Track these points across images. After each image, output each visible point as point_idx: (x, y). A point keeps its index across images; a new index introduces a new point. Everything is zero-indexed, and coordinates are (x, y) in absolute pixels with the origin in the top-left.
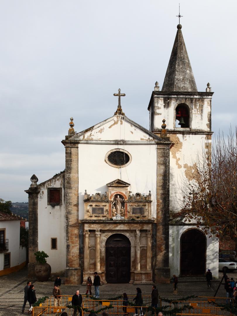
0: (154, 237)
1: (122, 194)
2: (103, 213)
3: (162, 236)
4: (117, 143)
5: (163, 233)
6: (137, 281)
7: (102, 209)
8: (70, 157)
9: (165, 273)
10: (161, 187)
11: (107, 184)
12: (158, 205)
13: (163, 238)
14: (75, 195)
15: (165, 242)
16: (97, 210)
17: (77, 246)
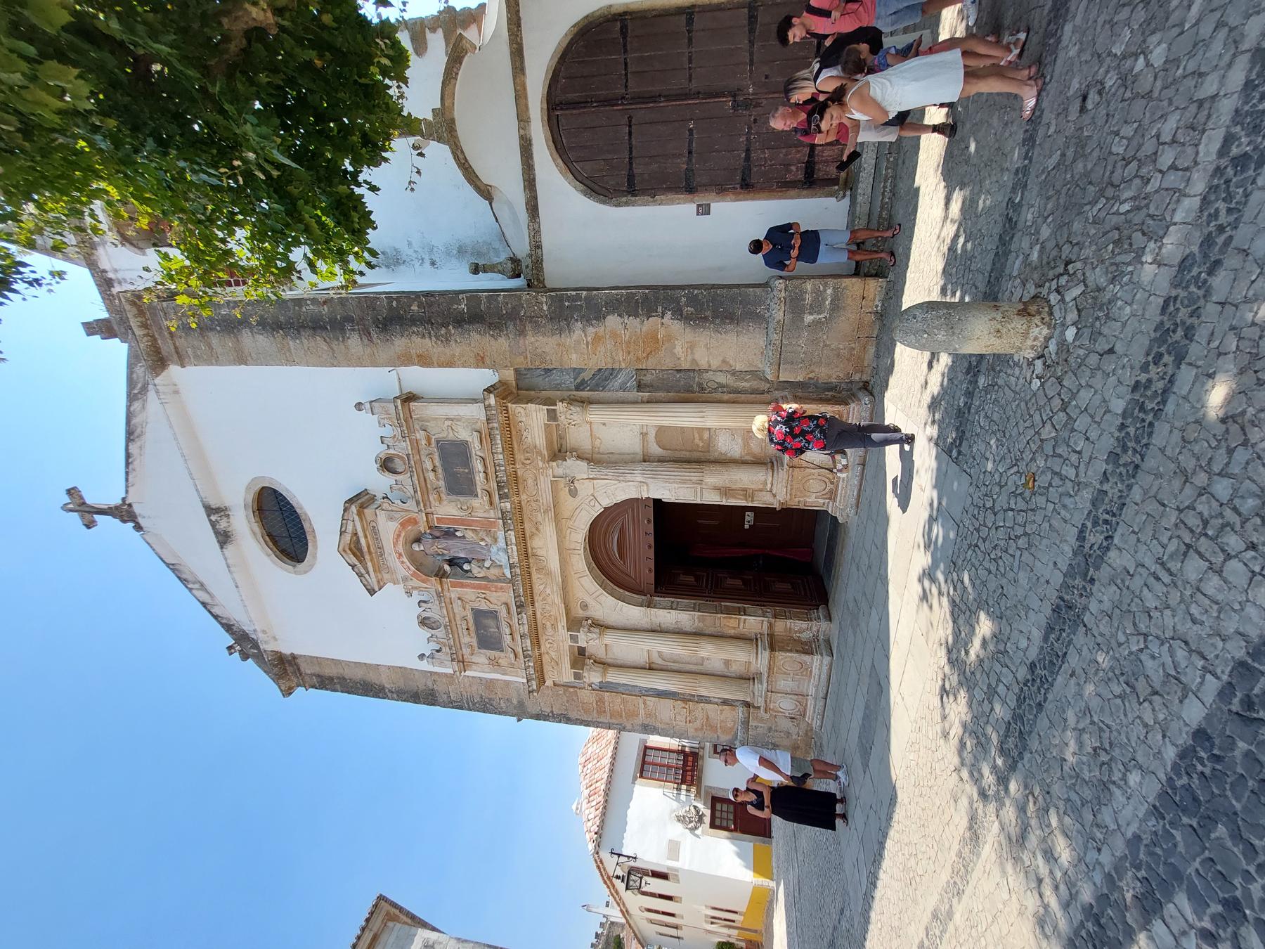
0: (590, 389)
1: (399, 536)
2: (493, 615)
3: (578, 334)
4: (224, 538)
5: (561, 331)
6: (832, 495)
7: (479, 615)
8: (331, 679)
9: (809, 318)
10: (334, 344)
11: (372, 592)
12: (425, 361)
13: (591, 330)
14: (451, 683)
15: (613, 321)
16: (486, 632)
17: (645, 703)
